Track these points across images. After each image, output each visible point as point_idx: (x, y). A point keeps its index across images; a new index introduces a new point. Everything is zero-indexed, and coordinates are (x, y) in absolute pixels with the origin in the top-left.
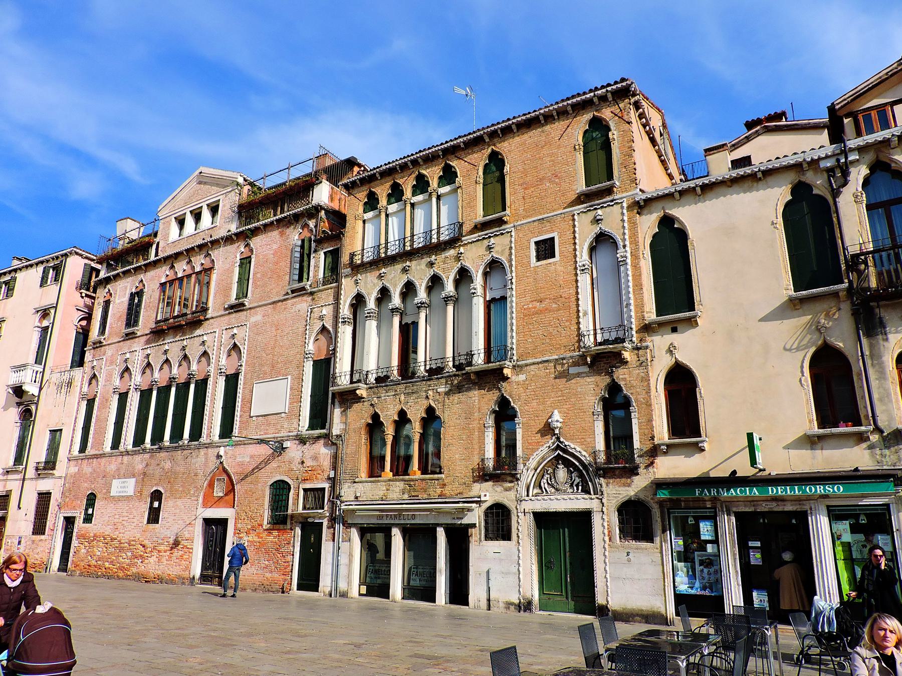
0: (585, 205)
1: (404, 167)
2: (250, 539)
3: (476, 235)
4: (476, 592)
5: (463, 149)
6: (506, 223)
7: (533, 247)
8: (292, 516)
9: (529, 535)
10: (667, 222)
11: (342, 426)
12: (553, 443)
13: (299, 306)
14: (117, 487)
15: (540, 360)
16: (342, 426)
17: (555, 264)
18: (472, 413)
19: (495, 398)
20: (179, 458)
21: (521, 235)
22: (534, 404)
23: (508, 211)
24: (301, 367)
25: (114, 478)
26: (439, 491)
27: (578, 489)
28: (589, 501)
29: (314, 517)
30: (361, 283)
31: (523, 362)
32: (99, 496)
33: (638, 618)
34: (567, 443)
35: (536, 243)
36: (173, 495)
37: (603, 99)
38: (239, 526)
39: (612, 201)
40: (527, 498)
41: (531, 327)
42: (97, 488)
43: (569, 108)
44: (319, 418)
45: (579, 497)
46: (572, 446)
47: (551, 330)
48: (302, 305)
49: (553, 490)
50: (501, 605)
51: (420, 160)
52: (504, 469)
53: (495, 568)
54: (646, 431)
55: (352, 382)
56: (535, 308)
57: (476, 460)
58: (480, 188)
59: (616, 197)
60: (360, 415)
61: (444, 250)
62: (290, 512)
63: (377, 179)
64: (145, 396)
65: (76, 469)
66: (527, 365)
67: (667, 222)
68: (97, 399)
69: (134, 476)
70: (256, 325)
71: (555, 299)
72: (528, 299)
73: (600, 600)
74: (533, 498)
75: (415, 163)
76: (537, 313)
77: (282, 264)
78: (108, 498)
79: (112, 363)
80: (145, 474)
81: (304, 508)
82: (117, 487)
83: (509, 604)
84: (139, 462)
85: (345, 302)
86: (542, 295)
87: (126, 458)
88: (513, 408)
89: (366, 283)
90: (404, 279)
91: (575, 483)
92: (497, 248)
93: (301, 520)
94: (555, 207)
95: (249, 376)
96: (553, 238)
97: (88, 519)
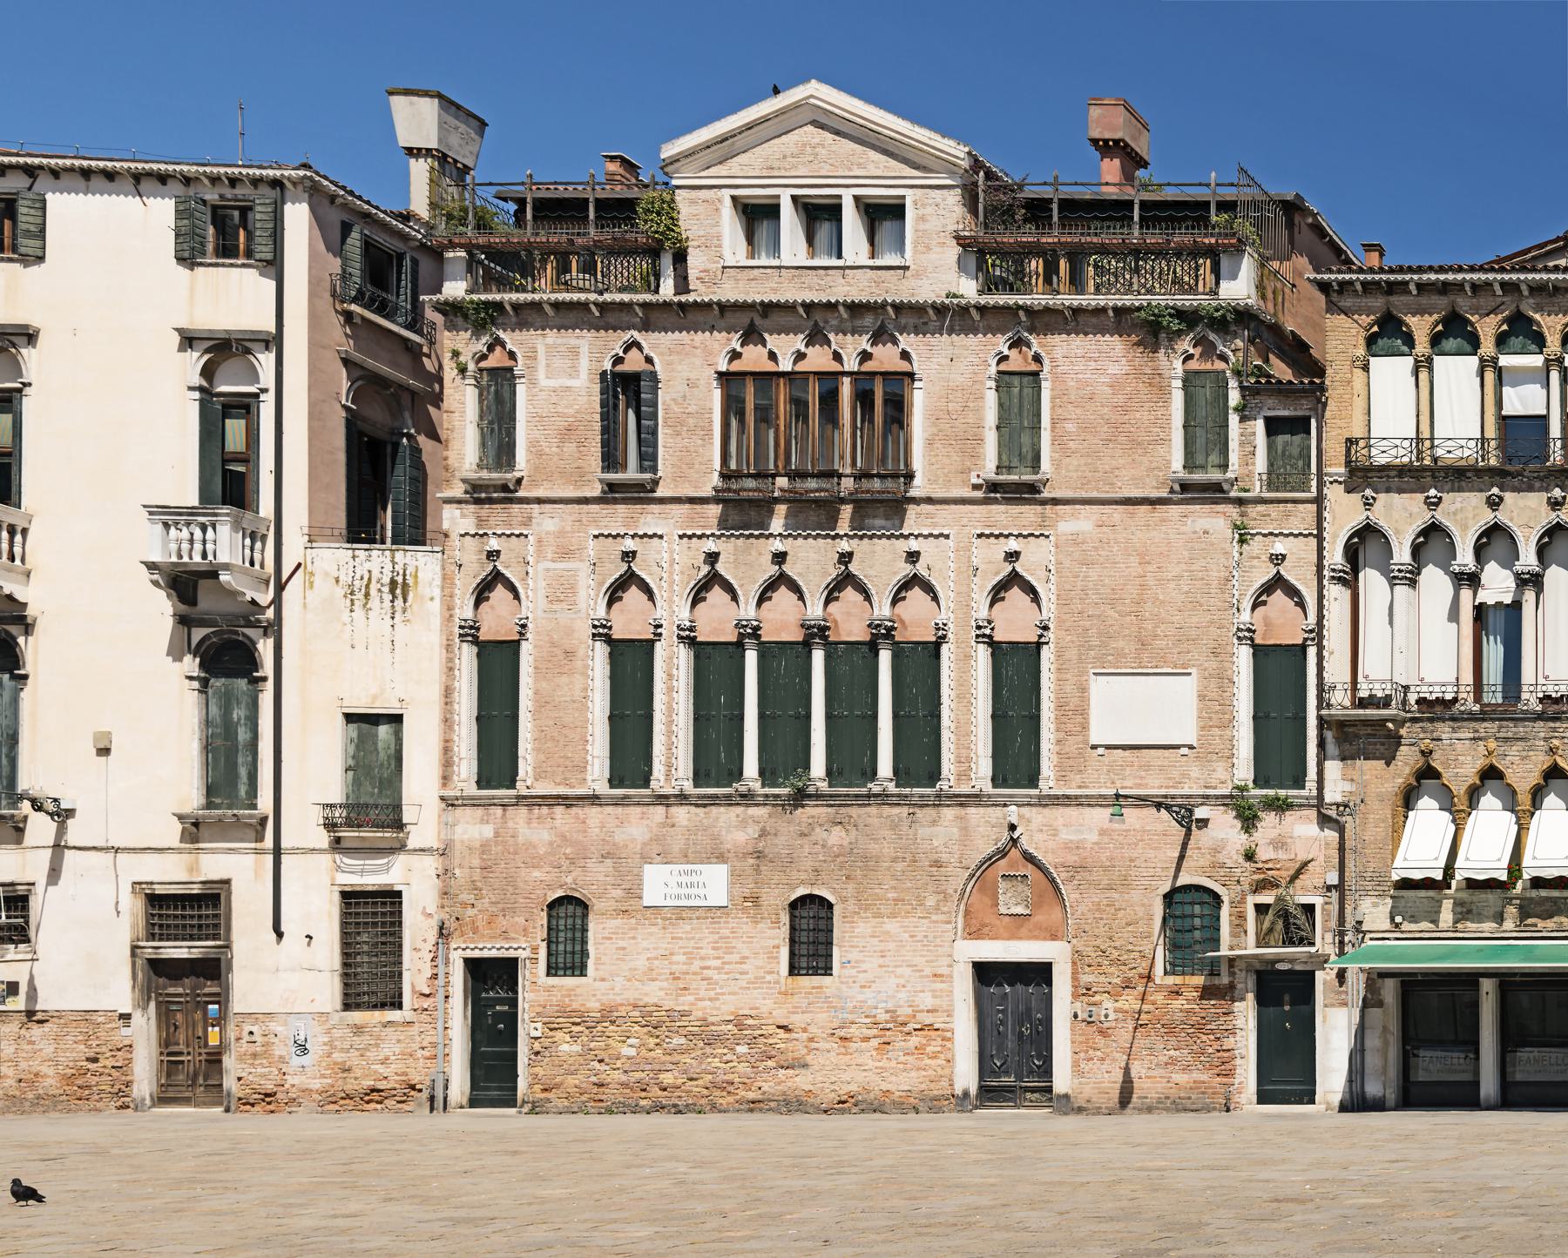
2: (1118, 1005)
8: (1232, 961)
14: (660, 884)
20: (875, 821)
25: (646, 859)
32: (597, 905)
36: (865, 905)
38: (1086, 979)
42: (591, 881)
48: (1214, 521)
64: (715, 664)
65: (488, 831)
68: (525, 647)
69: (721, 858)
70: (1076, 540)
78: (631, 904)
79: (565, 553)
80: (759, 855)
82: (660, 884)
84: (734, 825)
85: (1335, 536)
87: (681, 813)
90: (1487, 517)
95: (1072, 654)
97: (568, 956)
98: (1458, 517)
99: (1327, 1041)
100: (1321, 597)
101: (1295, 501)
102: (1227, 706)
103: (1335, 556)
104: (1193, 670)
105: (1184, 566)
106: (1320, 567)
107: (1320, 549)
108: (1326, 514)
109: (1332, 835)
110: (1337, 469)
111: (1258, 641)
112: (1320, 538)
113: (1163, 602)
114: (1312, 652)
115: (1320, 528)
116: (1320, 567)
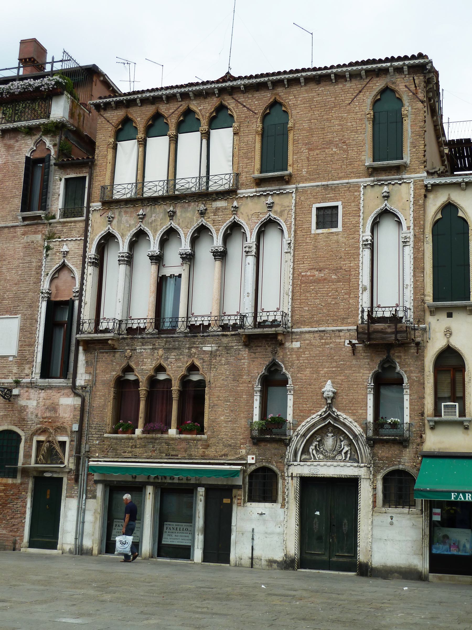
0: (372, 179)
1: (171, 98)
3: (254, 190)
4: (239, 550)
5: (243, 92)
6: (288, 183)
7: (314, 212)
9: (295, 498)
10: (450, 208)
11: (88, 377)
12: (325, 412)
13: (32, 237)
15: (316, 329)
16: (88, 377)
17: (337, 234)
18: (241, 376)
19: (267, 363)
21: (302, 198)
22: (308, 372)
23: (290, 170)
24: (33, 306)
26: (201, 451)
27: (346, 457)
28: (356, 469)
29: (51, 472)
30: (115, 222)
31: (298, 330)
33: (396, 575)
34: (339, 413)
35: (318, 209)
37: (399, 70)
39: (400, 179)
40: (295, 463)
43: (363, 73)
44: (55, 364)
45: (349, 464)
46: (345, 416)
47: (329, 300)
49: (321, 456)
50: (264, 563)
51: (191, 94)
52: (271, 432)
53: (259, 529)
54: (416, 407)
55: (97, 331)
56: (314, 276)
57: (243, 422)
58: (258, 139)
59: (404, 176)
61: (215, 200)
62: (20, 464)
63: (136, 105)
66: (302, 333)
67: (450, 208)
71: (336, 270)
72: (306, 266)
73: (362, 557)
74: (302, 463)
75: (185, 96)
76: (314, 282)
77: (9, 184)
81: (36, 462)
83: (271, 562)
85: (93, 240)
86: (321, 265)
88: (284, 374)
89: (119, 222)
91: (344, 451)
92: (276, 208)
93: (35, 474)
94: (340, 175)
96: (337, 207)
98: (153, 225)
99: (66, 516)
100: (83, 273)
101: (75, 222)
102: (33, 333)
103: (92, 252)
104: (19, 316)
105: (20, 261)
106: (84, 257)
107: (85, 247)
108: (89, 228)
109: (78, 401)
110: (96, 205)
111: (53, 299)
112: (86, 241)
113: (9, 280)
114: (77, 303)
115: (86, 236)
116: (84, 257)
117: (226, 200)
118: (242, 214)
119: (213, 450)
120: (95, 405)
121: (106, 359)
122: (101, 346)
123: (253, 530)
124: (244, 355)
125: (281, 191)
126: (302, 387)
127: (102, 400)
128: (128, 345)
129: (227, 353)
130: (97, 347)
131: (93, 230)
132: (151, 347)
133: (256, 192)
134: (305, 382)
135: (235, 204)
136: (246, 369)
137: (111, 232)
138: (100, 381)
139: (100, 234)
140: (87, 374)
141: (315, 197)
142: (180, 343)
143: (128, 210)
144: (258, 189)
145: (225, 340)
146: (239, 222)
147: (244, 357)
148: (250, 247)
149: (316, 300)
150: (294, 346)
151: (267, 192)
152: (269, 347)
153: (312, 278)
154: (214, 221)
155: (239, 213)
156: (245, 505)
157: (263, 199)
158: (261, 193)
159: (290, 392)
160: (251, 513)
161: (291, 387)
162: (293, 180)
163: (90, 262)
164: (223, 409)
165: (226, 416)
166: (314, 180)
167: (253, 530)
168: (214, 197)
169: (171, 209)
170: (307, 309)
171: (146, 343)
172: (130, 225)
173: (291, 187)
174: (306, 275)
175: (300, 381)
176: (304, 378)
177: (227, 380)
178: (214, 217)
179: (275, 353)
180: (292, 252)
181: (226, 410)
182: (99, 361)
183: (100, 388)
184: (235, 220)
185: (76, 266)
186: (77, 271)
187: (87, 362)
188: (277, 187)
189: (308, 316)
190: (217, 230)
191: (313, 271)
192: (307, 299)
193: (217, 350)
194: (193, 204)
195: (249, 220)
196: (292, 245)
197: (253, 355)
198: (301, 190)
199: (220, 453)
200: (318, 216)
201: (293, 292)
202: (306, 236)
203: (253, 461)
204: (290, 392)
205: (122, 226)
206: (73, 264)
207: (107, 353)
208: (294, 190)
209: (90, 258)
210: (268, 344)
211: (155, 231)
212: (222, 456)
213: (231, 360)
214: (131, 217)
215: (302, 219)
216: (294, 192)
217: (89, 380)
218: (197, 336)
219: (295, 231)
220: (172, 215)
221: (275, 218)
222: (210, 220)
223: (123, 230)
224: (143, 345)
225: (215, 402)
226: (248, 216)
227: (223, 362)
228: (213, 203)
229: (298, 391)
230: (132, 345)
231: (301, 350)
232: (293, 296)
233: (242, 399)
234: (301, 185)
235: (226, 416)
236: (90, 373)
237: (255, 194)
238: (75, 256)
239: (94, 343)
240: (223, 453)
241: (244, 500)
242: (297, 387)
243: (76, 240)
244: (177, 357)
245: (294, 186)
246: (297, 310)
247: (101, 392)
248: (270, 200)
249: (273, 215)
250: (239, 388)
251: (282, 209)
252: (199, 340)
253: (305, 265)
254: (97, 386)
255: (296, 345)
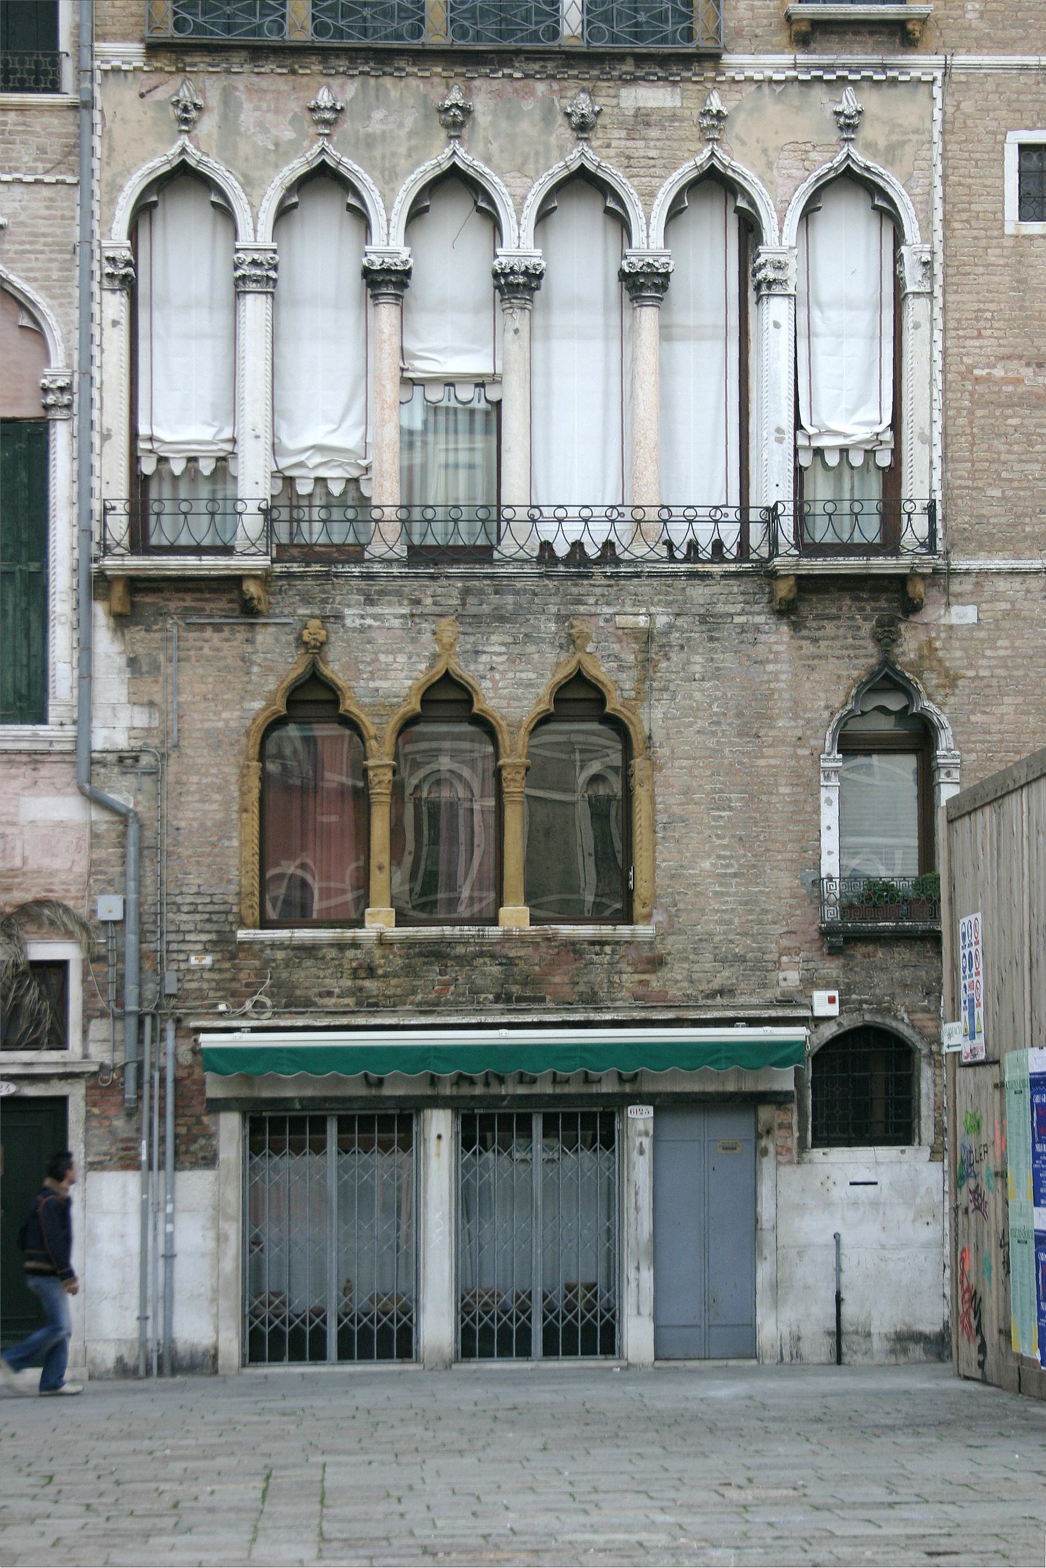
3: (787, 59)
16: (141, 718)
18: (765, 718)
21: (967, 107)
35: (1023, 148)
41: (1000, 446)
50: (877, 1344)
56: (1019, 381)
57: (782, 881)
60: (231, 685)
66: (984, 573)
92: (868, 132)
117: (675, 83)
118: (743, 143)
119: (679, 977)
120: (183, 824)
121: (218, 650)
122: (189, 603)
123: (837, 1237)
124: (775, 648)
125: (890, 74)
126: (990, 759)
127: (215, 806)
128: (306, 599)
129: (711, 639)
130: (172, 606)
131: (111, 149)
132: (405, 610)
133: (795, 67)
134: (1001, 741)
135: (715, 103)
136: (786, 696)
137: (192, 162)
138: (198, 735)
139: (145, 169)
140: (137, 709)
141: (1015, 105)
142: (523, 600)
143: (263, 83)
144: (802, 58)
145: (699, 593)
146: (730, 173)
147: (777, 653)
148: (779, 267)
149: (1027, 466)
150: (954, 620)
151: (840, 73)
152: (865, 619)
153: (1010, 388)
154: (629, 158)
155: (729, 137)
156: (806, 1157)
157: (819, 93)
158: (815, 73)
159: (948, 774)
160: (829, 1184)
161: (954, 757)
162: (932, 37)
163: (110, 276)
164: (708, 832)
165: (719, 857)
166: (1005, 46)
167: (837, 1237)
168: (625, 68)
169: (455, 97)
170: (997, 493)
171: (382, 593)
172: (277, 145)
173: (921, 63)
174: (988, 379)
175: (980, 737)
176: (994, 728)
177: (714, 734)
178: (630, 144)
179: (886, 637)
180: (938, 292)
181: (718, 836)
182: (187, 659)
183: (200, 761)
184: (715, 162)
185: (46, 288)
186: (50, 307)
187: (133, 663)
188: (875, 59)
189: (1003, 520)
190: (648, 195)
191: (1015, 364)
192: (998, 461)
193: (671, 626)
194: (541, 87)
195: (769, 165)
196: (938, 269)
197: (808, 648)
198: (963, 78)
199: (704, 987)
200: (1023, 173)
201: (945, 434)
202: (984, 243)
203: (834, 1010)
204: (948, 774)
205: (244, 149)
206: (27, 279)
207: (217, 628)
208: (938, 74)
209: (112, 260)
210: (861, 609)
211: (389, 178)
212: (712, 995)
213: (727, 660)
214: (277, 111)
215: (969, 181)
216: (939, 83)
217: (148, 730)
218: (587, 576)
219: (946, 221)
220: (457, 122)
221: (867, 169)
222: (612, 152)
223: (247, 159)
224: (370, 601)
225: (677, 810)
226: (765, 151)
227: (698, 668)
228: (624, 92)
229: (976, 771)
230: (324, 601)
231: (982, 634)
232: (945, 447)
233: (774, 799)
234: (961, 59)
235: (719, 857)
236: (151, 704)
237: (792, 73)
238: (39, 247)
239: (159, 590)
240: (716, 985)
241: (802, 1140)
242: (974, 756)
243: (37, 182)
244: (516, 649)
245: (939, 59)
246: (962, 497)
247: (207, 774)
248: (849, 101)
249: (861, 158)
250: (762, 762)
251: (894, 138)
252: (598, 591)
253: (986, 342)
254: (189, 751)
255: (963, 615)
